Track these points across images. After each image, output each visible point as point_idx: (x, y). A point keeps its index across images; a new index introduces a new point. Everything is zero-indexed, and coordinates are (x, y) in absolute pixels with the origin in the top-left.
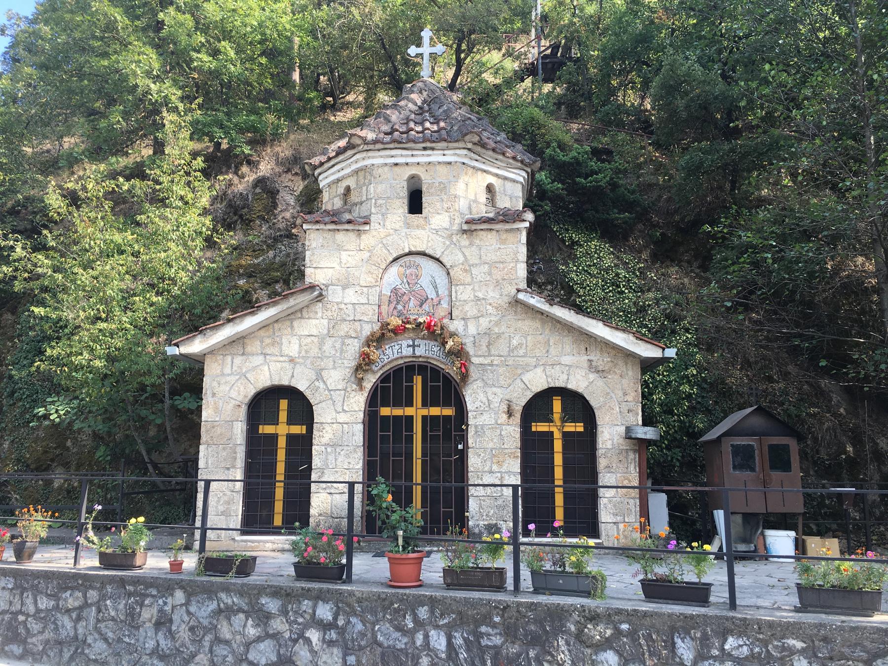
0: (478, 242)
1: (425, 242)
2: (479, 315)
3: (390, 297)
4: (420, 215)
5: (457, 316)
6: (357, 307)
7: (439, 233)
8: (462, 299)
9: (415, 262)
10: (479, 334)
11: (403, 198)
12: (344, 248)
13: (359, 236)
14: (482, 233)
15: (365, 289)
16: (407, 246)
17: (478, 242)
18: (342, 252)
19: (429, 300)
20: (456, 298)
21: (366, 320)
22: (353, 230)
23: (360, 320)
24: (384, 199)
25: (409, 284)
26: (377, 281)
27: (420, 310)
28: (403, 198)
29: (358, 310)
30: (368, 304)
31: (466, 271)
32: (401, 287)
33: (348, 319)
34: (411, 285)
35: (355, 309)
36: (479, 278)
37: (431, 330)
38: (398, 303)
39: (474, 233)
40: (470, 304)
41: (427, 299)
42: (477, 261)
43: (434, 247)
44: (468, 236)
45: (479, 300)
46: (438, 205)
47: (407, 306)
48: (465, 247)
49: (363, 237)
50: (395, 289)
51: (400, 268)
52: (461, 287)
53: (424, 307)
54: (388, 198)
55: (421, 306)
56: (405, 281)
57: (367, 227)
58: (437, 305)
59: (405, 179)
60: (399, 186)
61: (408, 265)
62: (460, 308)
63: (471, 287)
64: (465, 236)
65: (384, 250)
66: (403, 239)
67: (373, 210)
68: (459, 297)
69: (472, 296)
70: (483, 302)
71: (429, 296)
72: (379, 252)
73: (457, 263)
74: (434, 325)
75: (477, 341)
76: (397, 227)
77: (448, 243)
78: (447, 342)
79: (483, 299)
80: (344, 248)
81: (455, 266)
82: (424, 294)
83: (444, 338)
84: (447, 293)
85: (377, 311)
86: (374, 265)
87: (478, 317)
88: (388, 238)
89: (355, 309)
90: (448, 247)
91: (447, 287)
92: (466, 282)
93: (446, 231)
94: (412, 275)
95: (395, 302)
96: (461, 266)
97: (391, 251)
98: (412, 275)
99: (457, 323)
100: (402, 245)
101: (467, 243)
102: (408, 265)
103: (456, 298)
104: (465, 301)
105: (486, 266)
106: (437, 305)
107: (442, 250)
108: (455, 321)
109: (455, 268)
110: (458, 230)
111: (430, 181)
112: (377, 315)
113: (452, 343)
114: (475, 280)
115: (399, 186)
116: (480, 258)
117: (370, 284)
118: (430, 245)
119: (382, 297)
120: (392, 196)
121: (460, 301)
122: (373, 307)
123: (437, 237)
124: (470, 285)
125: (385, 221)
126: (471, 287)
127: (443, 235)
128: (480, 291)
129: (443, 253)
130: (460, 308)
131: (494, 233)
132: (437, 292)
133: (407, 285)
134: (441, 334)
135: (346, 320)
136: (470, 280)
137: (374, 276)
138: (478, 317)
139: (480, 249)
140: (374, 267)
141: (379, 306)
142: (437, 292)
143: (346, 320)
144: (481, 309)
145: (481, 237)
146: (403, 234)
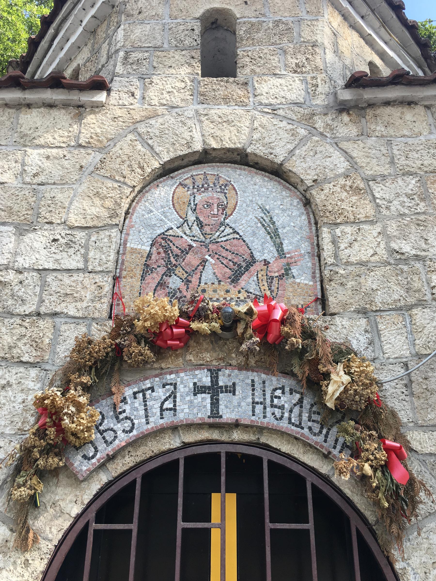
0: (380, 128)
1: (246, 131)
2: (411, 300)
3: (149, 256)
4: (231, 79)
5: (345, 306)
6: (50, 278)
7: (281, 112)
8: (353, 259)
9: (218, 177)
10: (420, 356)
11: (191, 48)
12: (36, 142)
13: (79, 117)
14: (388, 110)
15: (80, 235)
16: (197, 136)
17: (380, 128)
18: (29, 151)
19: (257, 266)
20: (336, 256)
21: (72, 312)
22: (66, 105)
23: (55, 314)
24: (147, 49)
25: (201, 225)
26: (113, 216)
27: (233, 294)
28: (191, 48)
29: (54, 286)
30: (84, 270)
31: (357, 190)
32: (179, 232)
33: (20, 310)
34: (207, 229)
35: (44, 285)
36: (395, 205)
37: (271, 338)
38: (169, 272)
39: (370, 112)
40: (379, 273)
41: (252, 261)
42: (385, 170)
43: (267, 140)
44: (354, 117)
45: (406, 261)
46: (275, 60)
47: (194, 280)
48: (349, 140)
49: (90, 119)
50: (164, 236)
51: (181, 189)
52: (348, 229)
53: (242, 282)
54: (157, 48)
55: (235, 280)
56: (192, 218)
57: (102, 97)
58: (281, 277)
59: (198, 15)
60: (182, 27)
61: (199, 183)
62: (350, 284)
63: (378, 228)
64: (345, 118)
65: (139, 147)
66: (189, 123)
67: (119, 69)
68: (344, 255)
69: (382, 251)
70: (418, 265)
71: (258, 256)
72: (127, 150)
73: (330, 175)
74: (283, 321)
75: (416, 377)
76: (176, 100)
77: (302, 132)
78: (327, 376)
79: (417, 257)
80: (36, 142)
81: (326, 180)
82: (243, 250)
83: (316, 362)
84: (305, 247)
85: (107, 288)
86: (111, 178)
87: (410, 308)
88: (152, 121)
89: (44, 285)
90: (303, 141)
91: (305, 232)
92: (362, 217)
93: (296, 109)
94: (209, 205)
95: (162, 270)
96: (342, 181)
97: (158, 149)
98: (209, 205)
99: (346, 322)
100: (187, 135)
101: (353, 131)
102: (199, 183)
103: (336, 256)
104: (361, 264)
105: (413, 181)
106: (281, 277)
107: (290, 147)
108: (338, 320)
109: (327, 186)
110: (326, 107)
111: (253, 20)
112: (106, 301)
113: (346, 379)
114: (385, 212)
115: (182, 27)
116: (392, 162)
117: (96, 223)
118: (256, 136)
119: (128, 257)
120: (166, 46)
121: (348, 263)
122: (98, 278)
123: (275, 121)
124: (372, 223)
125: (145, 89)
126: (378, 228)
127: (290, 115)
128: (405, 237)
129: (291, 152)
130: (350, 284)
131: (419, 110)
132: (279, 247)
133: (195, 228)
134: (304, 350)
135: (12, 315)
136: (372, 212)
137: (109, 203)
138: (410, 308)
139: (389, 143)
140: (110, 183)
141: (116, 279)
142: (279, 247)
143: (12, 315)
144: (417, 285)
145: (386, 118)
146: (191, 113)
